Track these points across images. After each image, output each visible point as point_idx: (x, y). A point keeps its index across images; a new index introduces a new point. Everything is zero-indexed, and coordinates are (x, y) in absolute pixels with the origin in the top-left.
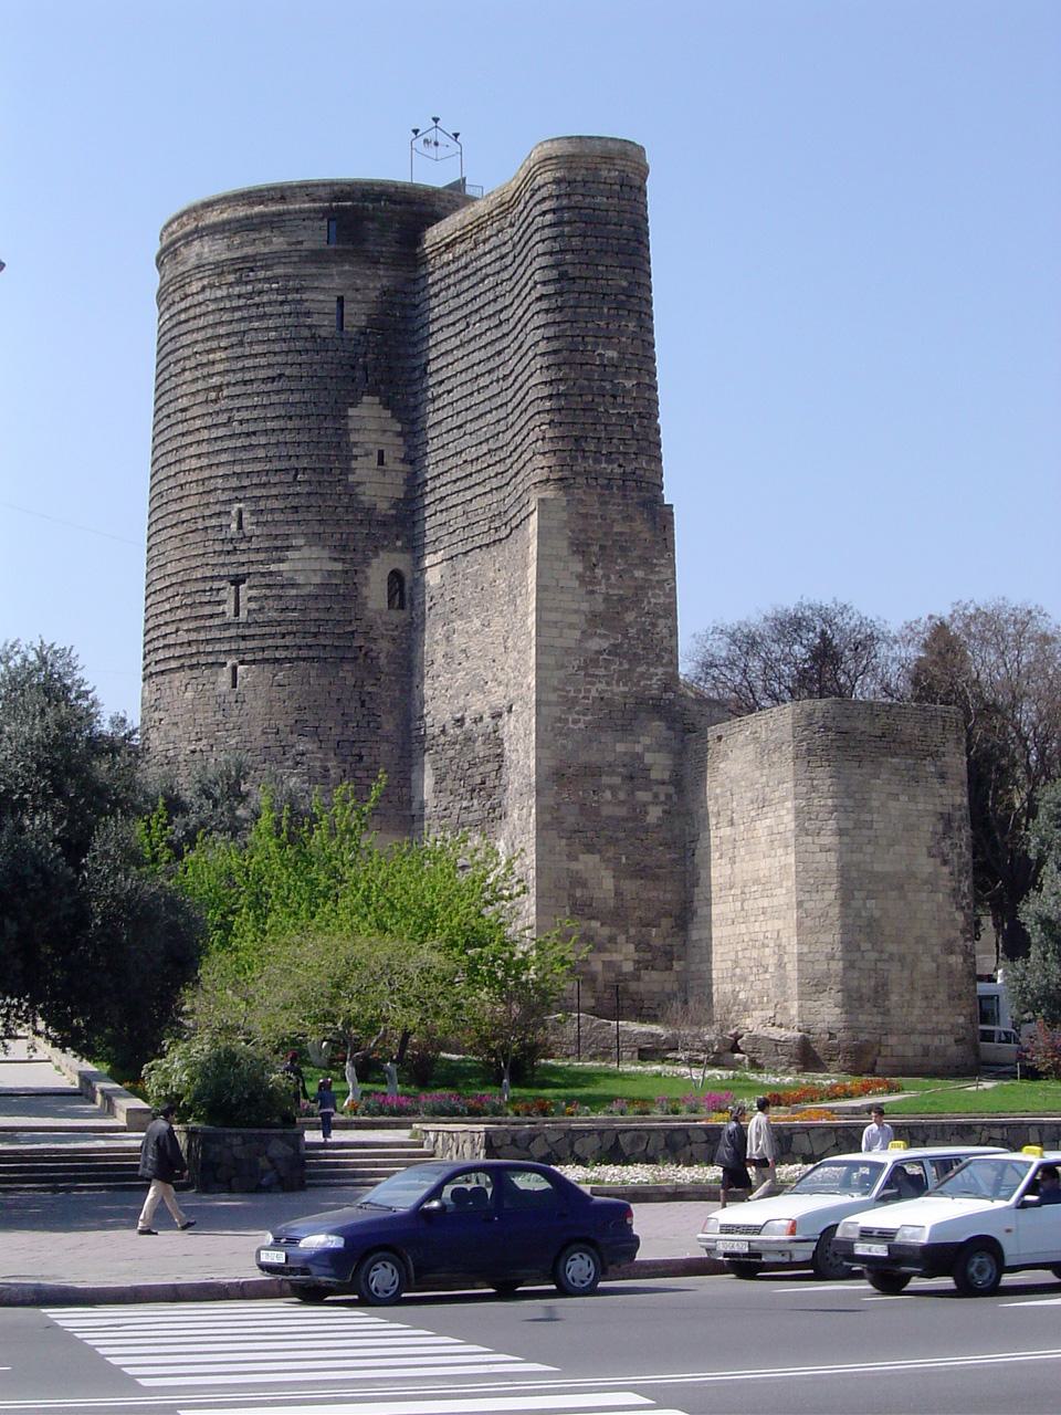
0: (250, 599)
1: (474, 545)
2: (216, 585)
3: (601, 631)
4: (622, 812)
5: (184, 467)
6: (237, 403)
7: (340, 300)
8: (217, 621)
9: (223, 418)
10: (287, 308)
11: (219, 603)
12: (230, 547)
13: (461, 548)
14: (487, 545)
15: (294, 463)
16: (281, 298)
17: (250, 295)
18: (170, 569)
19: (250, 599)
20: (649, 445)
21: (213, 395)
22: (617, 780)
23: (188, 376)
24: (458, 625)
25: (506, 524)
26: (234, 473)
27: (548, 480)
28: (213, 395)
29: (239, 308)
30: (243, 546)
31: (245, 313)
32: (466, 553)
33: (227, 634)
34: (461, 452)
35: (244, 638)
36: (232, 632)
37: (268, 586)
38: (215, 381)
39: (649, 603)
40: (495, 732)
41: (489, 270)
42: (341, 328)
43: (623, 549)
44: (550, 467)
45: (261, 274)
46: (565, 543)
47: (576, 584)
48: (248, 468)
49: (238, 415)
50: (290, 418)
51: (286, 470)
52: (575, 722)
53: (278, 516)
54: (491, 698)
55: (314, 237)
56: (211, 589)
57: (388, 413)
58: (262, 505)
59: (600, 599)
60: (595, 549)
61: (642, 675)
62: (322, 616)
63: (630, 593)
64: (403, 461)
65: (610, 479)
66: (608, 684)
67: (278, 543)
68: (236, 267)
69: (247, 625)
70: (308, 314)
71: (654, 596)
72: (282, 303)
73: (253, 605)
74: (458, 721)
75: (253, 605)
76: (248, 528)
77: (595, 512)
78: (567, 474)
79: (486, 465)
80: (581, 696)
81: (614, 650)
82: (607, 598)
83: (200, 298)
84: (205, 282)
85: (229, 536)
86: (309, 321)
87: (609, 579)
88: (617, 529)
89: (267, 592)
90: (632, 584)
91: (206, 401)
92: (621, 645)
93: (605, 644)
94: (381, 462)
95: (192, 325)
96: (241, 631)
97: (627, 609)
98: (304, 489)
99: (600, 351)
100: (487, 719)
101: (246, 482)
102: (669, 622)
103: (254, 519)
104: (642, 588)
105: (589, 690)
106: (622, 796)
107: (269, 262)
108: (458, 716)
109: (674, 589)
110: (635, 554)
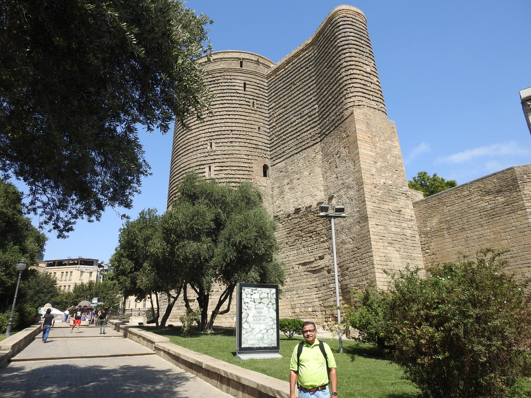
2: (201, 167)
4: (398, 230)
7: (245, 84)
12: (207, 154)
13: (296, 151)
14: (309, 147)
17: (214, 81)
22: (395, 217)
26: (209, 132)
32: (297, 153)
37: (222, 167)
41: (302, 66)
44: (354, 101)
45: (219, 75)
53: (225, 144)
54: (317, 198)
55: (236, 65)
59: (379, 148)
67: (225, 153)
72: (225, 83)
78: (360, 103)
80: (378, 183)
87: (380, 142)
93: (383, 165)
98: (235, 136)
101: (213, 134)
110: (386, 135)
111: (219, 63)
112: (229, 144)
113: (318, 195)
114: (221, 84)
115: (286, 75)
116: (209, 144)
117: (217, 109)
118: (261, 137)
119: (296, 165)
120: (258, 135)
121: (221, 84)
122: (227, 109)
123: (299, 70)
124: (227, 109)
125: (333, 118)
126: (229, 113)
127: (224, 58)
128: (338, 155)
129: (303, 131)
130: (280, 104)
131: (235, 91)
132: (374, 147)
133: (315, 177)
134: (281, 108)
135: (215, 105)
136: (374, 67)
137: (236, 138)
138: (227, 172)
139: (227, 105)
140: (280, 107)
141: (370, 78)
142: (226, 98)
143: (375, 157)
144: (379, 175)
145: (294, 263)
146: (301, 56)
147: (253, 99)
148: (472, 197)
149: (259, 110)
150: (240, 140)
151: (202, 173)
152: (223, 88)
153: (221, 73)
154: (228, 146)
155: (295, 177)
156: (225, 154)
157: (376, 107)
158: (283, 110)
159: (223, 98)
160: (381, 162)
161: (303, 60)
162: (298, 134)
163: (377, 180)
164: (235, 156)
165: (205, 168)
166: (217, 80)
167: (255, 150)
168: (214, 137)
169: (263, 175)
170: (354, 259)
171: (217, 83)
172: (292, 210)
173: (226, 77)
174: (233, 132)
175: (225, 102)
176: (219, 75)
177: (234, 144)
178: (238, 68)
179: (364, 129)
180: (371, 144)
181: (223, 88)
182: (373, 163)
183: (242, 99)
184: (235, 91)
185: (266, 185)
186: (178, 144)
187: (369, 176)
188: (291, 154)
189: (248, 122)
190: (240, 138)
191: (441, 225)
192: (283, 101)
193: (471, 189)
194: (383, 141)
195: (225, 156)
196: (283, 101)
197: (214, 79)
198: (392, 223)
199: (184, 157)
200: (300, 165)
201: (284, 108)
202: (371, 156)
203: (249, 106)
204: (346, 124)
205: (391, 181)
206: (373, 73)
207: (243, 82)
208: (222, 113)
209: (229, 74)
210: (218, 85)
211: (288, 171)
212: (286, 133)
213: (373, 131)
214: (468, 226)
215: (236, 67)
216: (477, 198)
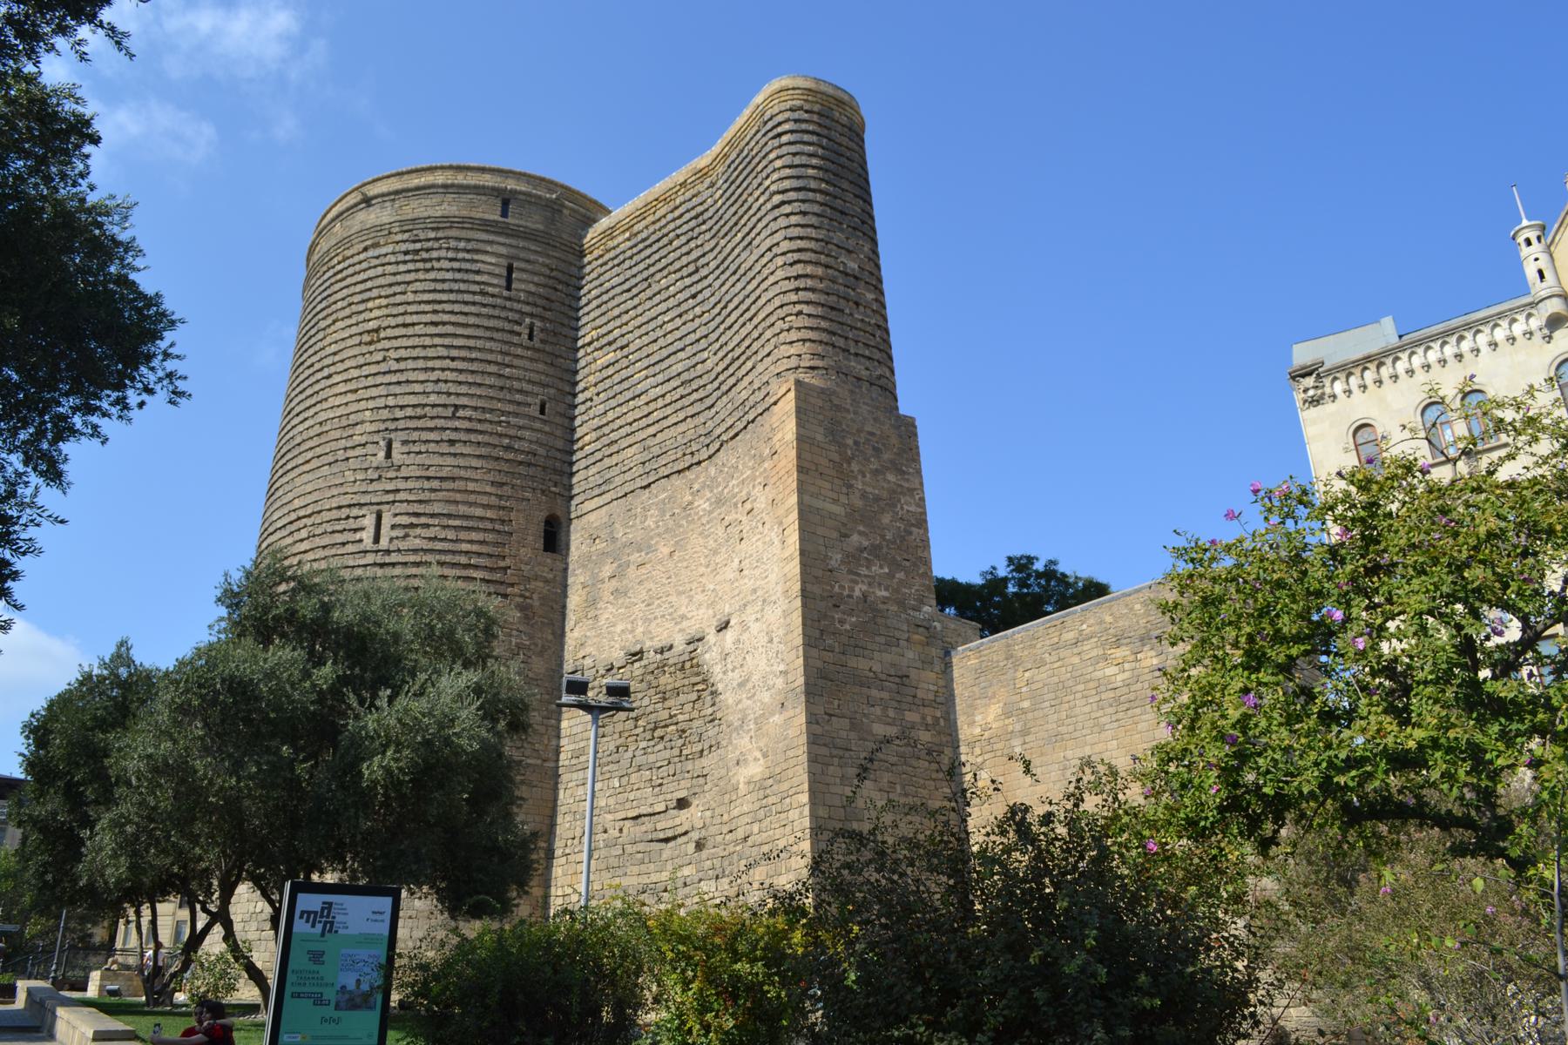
0: (393, 527)
1: (661, 475)
2: (355, 512)
3: (861, 528)
5: (325, 405)
6: (395, 343)
7: (510, 269)
8: (350, 548)
9: (379, 357)
10: (456, 265)
11: (355, 530)
14: (679, 472)
15: (453, 400)
16: (450, 255)
17: (416, 252)
18: (297, 504)
19: (393, 527)
20: (887, 358)
21: (366, 338)
22: (885, 695)
23: (340, 325)
24: (636, 557)
25: (708, 446)
27: (796, 368)
28: (366, 338)
29: (405, 262)
30: (391, 474)
31: (411, 266)
33: (362, 562)
34: (639, 396)
35: (382, 565)
36: (370, 559)
37: (417, 515)
38: (372, 325)
39: (902, 508)
40: (692, 659)
41: (679, 232)
42: (509, 288)
43: (875, 449)
44: (800, 356)
45: (432, 235)
46: (821, 430)
47: (834, 473)
48: (401, 401)
49: (392, 354)
50: (453, 359)
51: (445, 406)
52: (842, 622)
53: (432, 447)
54: (685, 624)
56: (348, 517)
57: (551, 371)
58: (415, 436)
59: (858, 494)
60: (850, 442)
61: (901, 581)
62: (475, 548)
63: (885, 495)
64: (563, 415)
65: (859, 379)
66: (870, 584)
67: (431, 473)
68: (406, 228)
69: (388, 552)
70: (478, 272)
71: (907, 503)
72: (451, 260)
73: (395, 533)
74: (634, 655)
75: (399, 533)
76: (395, 453)
77: (848, 406)
79: (678, 396)
80: (846, 593)
81: (875, 550)
82: (864, 495)
83: (362, 257)
84: (369, 243)
85: (374, 465)
86: (478, 278)
87: (864, 476)
88: (868, 428)
89: (414, 520)
90: (886, 485)
91: (360, 344)
92: (879, 547)
93: (866, 543)
94: (542, 412)
95: (349, 281)
96: (379, 559)
97: (883, 511)
98: (466, 425)
99: (842, 259)
100: (680, 646)
101: (399, 414)
102: (922, 532)
103: (405, 449)
104: (894, 492)
105: (852, 590)
106: (891, 713)
107: (441, 225)
108: (638, 648)
109: (922, 499)
110: (886, 456)
111: (436, 199)
112: (445, 448)
113: (689, 615)
114: (436, 265)
115: (635, 250)
116: (382, 443)
117: (417, 339)
118: (547, 429)
119: (638, 521)
120: (538, 425)
121: (436, 265)
122: (447, 341)
123: (671, 243)
124: (447, 341)
125: (744, 395)
126: (454, 353)
127: (452, 186)
128: (748, 506)
129: (665, 423)
130: (610, 337)
131: (476, 288)
132: (844, 490)
133: (685, 564)
134: (614, 346)
135: (413, 324)
136: (870, 259)
137: (468, 431)
138: (430, 533)
139: (449, 329)
140: (610, 344)
141: (854, 290)
142: (448, 307)
143: (845, 520)
144: (850, 572)
145: (610, 817)
146: (678, 202)
147: (531, 315)
148: (1085, 648)
149: (548, 348)
150: (480, 438)
151: (355, 530)
152: (441, 275)
153: (438, 229)
154: (442, 454)
155: (632, 558)
156: (428, 478)
157: (865, 373)
158: (619, 354)
159: (437, 307)
160: (860, 533)
161: (682, 215)
162: (652, 430)
163: (842, 587)
164: (459, 485)
165: (364, 516)
166: (427, 250)
167: (522, 470)
168: (401, 424)
169: (542, 547)
170: (762, 812)
171: (424, 260)
172: (617, 656)
173: (453, 244)
174: (461, 413)
175: (446, 318)
176: (432, 235)
177: (459, 448)
178: (492, 217)
179: (819, 437)
180: (836, 481)
181: (441, 275)
182: (835, 535)
183: (496, 312)
184: (476, 288)
185: (550, 576)
186: (291, 434)
187: (820, 573)
188: (627, 488)
189: (508, 383)
190: (481, 432)
191: (1007, 722)
192: (620, 327)
193: (1084, 626)
194: (876, 473)
195: (427, 485)
196: (620, 327)
197: (418, 246)
198: (878, 710)
199: (306, 478)
200: (650, 523)
201: (622, 348)
202: (832, 516)
203: (519, 334)
204: (774, 419)
205: (886, 589)
206: (866, 276)
207: (504, 262)
208: (431, 353)
209: (463, 234)
210: (428, 265)
211: (614, 540)
212: (619, 423)
213: (846, 446)
214: (1071, 728)
215: (487, 216)
216: (1094, 653)
